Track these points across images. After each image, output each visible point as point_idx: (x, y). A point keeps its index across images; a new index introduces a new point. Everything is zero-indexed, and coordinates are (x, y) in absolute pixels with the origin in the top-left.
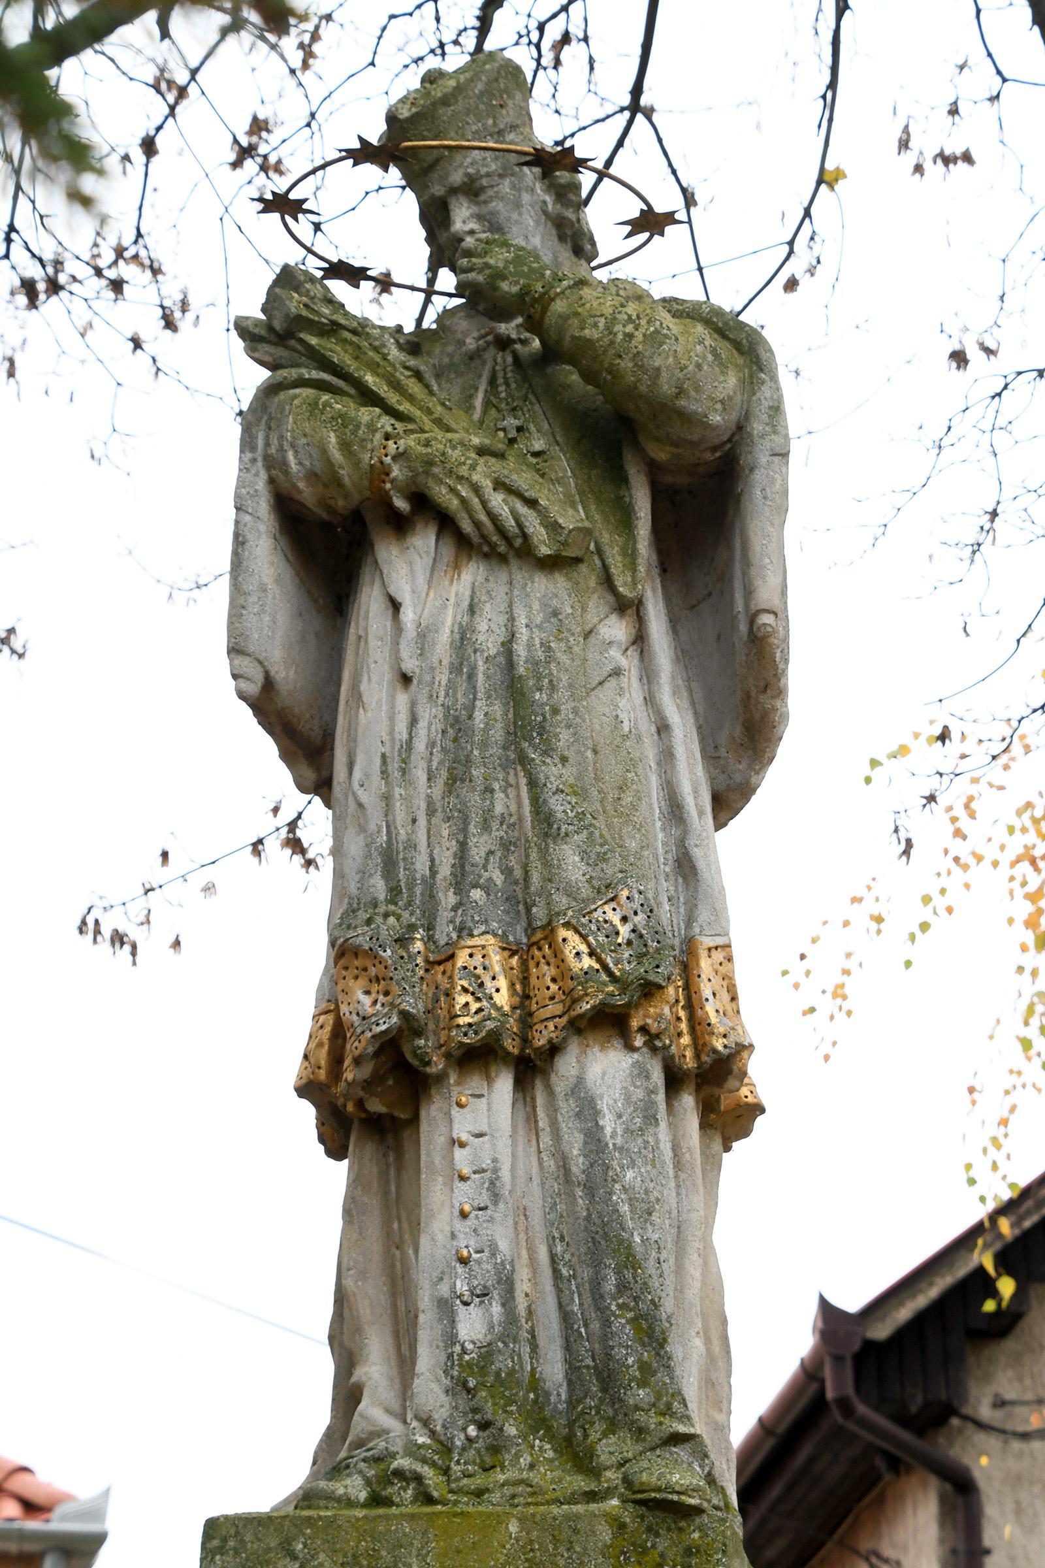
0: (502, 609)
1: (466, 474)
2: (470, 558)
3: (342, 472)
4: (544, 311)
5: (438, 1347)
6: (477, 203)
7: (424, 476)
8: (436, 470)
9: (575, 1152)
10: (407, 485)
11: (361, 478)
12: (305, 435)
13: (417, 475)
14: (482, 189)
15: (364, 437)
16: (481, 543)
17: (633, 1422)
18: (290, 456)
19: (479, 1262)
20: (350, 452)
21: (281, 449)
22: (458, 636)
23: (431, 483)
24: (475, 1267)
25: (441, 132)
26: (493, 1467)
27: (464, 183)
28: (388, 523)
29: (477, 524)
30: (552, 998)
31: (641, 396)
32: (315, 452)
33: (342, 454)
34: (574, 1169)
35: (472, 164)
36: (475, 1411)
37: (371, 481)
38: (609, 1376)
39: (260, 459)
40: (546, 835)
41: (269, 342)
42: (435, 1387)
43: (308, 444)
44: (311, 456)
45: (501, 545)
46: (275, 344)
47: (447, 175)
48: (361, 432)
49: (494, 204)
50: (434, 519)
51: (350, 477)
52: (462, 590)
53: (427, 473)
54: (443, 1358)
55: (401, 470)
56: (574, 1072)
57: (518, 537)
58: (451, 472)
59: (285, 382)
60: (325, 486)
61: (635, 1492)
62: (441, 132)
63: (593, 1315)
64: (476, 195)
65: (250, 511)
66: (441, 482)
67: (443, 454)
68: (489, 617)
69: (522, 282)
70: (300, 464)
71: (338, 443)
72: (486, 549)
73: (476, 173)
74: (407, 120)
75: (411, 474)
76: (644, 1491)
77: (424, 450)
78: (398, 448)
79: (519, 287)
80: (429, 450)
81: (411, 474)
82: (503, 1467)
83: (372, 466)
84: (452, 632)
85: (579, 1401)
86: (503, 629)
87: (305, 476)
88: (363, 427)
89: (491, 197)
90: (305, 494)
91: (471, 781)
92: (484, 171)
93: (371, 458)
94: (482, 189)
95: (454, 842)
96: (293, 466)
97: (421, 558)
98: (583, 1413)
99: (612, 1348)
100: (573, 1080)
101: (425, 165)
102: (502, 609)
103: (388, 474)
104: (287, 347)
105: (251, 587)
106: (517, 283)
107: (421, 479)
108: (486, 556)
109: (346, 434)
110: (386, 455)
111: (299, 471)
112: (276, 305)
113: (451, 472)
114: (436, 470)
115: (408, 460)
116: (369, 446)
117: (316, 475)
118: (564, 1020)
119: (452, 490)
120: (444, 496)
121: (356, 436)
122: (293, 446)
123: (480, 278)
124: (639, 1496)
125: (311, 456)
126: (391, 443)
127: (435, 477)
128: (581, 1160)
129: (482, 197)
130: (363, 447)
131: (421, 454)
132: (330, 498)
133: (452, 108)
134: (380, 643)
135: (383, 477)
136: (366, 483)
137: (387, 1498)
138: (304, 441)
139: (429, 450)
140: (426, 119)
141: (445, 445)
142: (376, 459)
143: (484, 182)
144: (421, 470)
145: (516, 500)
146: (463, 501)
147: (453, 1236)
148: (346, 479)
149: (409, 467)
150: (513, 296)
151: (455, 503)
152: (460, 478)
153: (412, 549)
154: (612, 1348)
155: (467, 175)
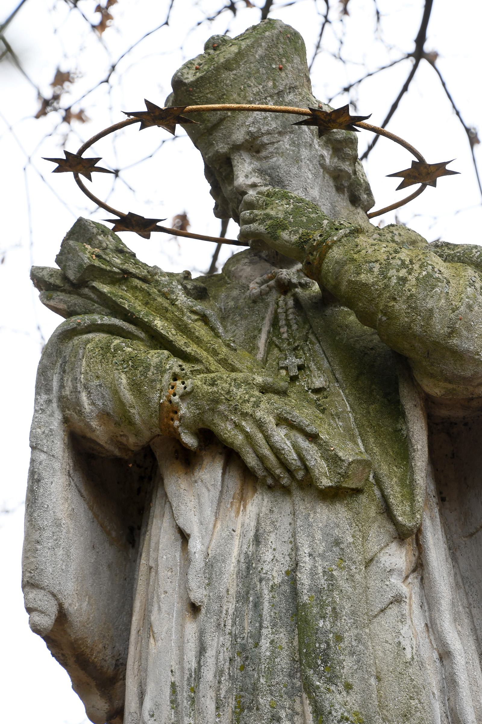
0: (286, 539)
1: (250, 411)
2: (255, 491)
3: (132, 411)
4: (322, 258)
6: (260, 159)
7: (210, 413)
8: (222, 407)
10: (195, 421)
11: (151, 416)
12: (98, 377)
13: (203, 412)
14: (264, 146)
15: (153, 377)
16: (265, 476)
18: (84, 396)
20: (141, 393)
21: (75, 391)
22: (244, 566)
23: (217, 420)
25: (224, 94)
27: (246, 140)
28: (177, 458)
32: (107, 393)
33: (133, 395)
35: (253, 123)
37: (160, 419)
39: (55, 400)
43: (100, 386)
44: (103, 397)
45: (284, 478)
46: (70, 293)
47: (231, 134)
48: (150, 373)
49: (275, 159)
50: (221, 454)
51: (140, 416)
52: (247, 521)
55: (188, 408)
57: (301, 469)
58: (236, 409)
59: (79, 328)
60: (117, 424)
62: (224, 94)
64: (258, 152)
65: (45, 449)
66: (227, 418)
67: (228, 392)
68: (273, 547)
69: (301, 231)
70: (93, 404)
71: (129, 384)
72: (270, 481)
73: (257, 131)
74: (192, 84)
75: (198, 412)
77: (210, 389)
78: (185, 388)
79: (298, 236)
80: (215, 389)
81: (198, 412)
83: (161, 405)
84: (239, 561)
86: (288, 558)
87: (97, 416)
88: (152, 369)
89: (272, 152)
90: (98, 432)
92: (264, 129)
93: (160, 397)
94: (264, 146)
96: (86, 406)
97: (209, 490)
101: (209, 125)
102: (286, 539)
103: (176, 412)
105: (46, 523)
107: (208, 416)
109: (136, 376)
110: (175, 395)
111: (92, 411)
112: (70, 256)
113: (236, 409)
114: (222, 407)
115: (195, 398)
116: (158, 386)
117: (108, 414)
119: (237, 426)
120: (229, 432)
121: (146, 377)
122: (86, 387)
123: (262, 228)
125: (103, 397)
126: (178, 383)
129: (264, 154)
130: (153, 388)
131: (207, 393)
132: (121, 436)
133: (234, 72)
134: (169, 573)
135: (172, 415)
136: (155, 421)
139: (215, 389)
140: (210, 83)
141: (230, 384)
142: (165, 398)
143: (265, 139)
144: (207, 408)
145: (298, 435)
148: (137, 417)
149: (196, 405)
150: (293, 244)
152: (244, 415)
153: (200, 483)
155: (249, 133)
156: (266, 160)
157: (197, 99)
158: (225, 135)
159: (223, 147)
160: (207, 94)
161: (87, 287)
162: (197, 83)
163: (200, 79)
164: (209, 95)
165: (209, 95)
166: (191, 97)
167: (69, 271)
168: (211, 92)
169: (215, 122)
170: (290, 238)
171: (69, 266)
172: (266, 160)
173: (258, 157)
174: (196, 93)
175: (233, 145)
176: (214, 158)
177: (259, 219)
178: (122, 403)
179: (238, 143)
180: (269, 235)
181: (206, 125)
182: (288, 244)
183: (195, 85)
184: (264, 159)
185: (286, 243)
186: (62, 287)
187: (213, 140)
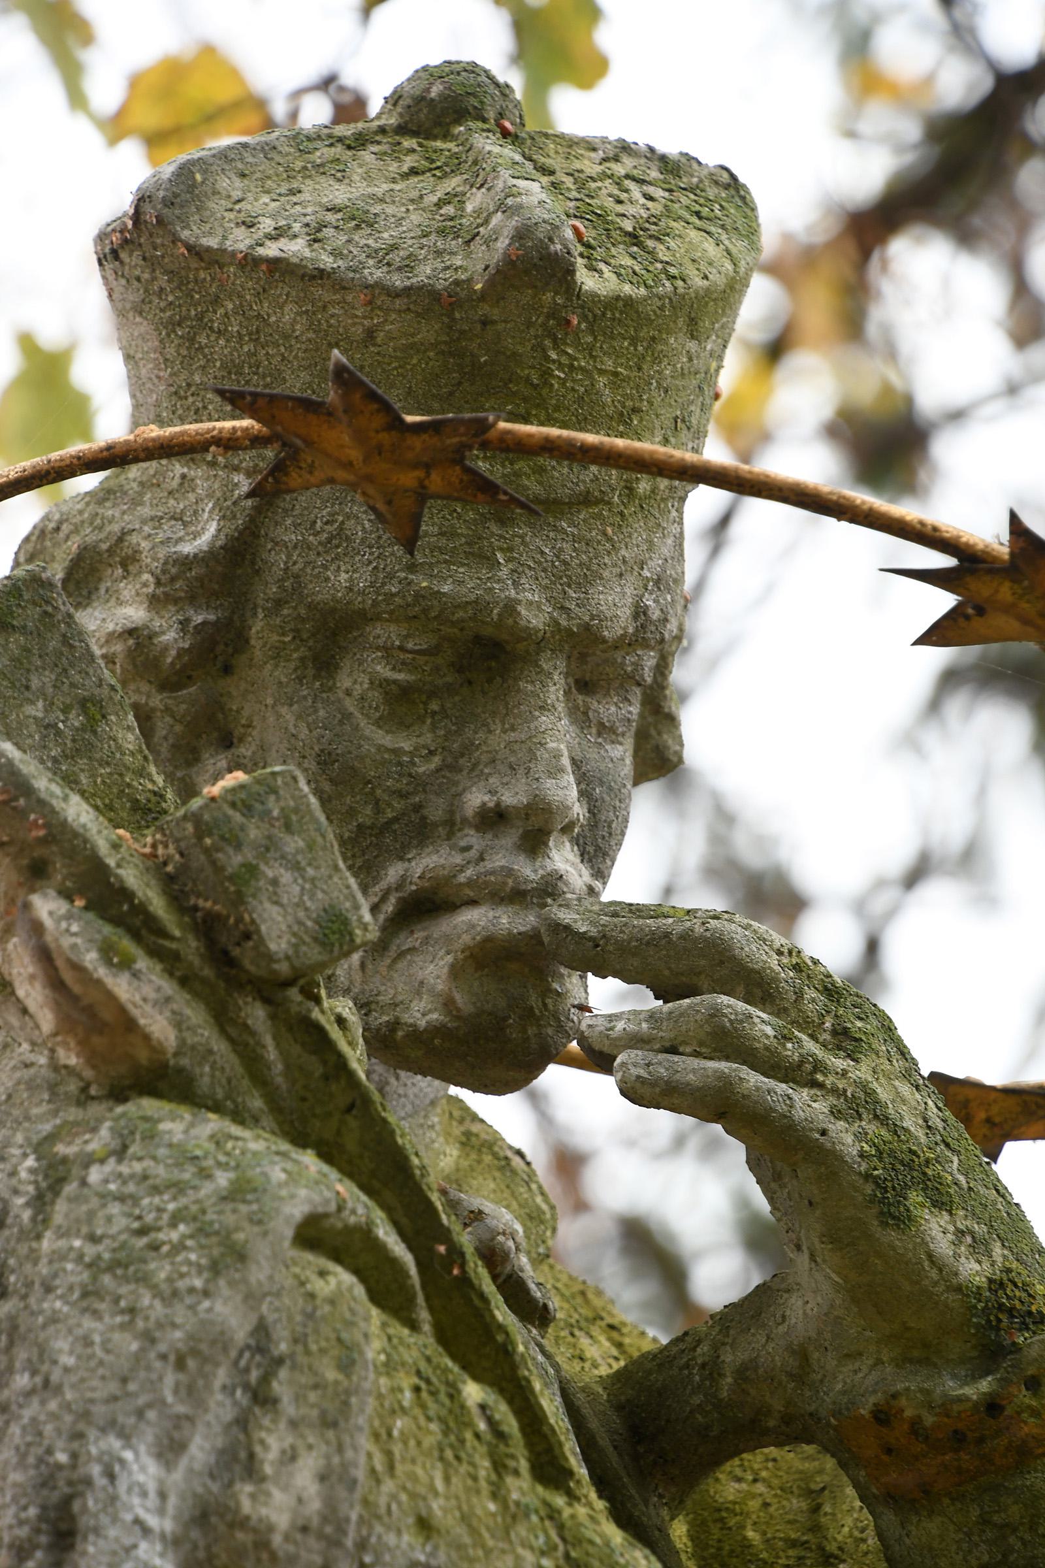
106: (979, 1247)
112: (293, 844)
140: (634, 341)
150: (959, 1289)
156: (599, 734)
157: (561, 367)
158: (565, 563)
159: (539, 606)
160: (602, 372)
161: (267, 1001)
162: (604, 314)
163: (620, 304)
164: (602, 381)
165: (602, 381)
166: (548, 343)
167: (267, 905)
168: (616, 374)
169: (563, 493)
170: (956, 1256)
171: (275, 882)
172: (599, 734)
173: (577, 708)
174: (577, 344)
175: (587, 627)
176: (460, 614)
177: (834, 1091)
179: (606, 633)
180: (869, 1189)
181: (517, 474)
182: (934, 1274)
183: (595, 316)
184: (594, 730)
185: (926, 1264)
186: (172, 938)
187: (501, 549)
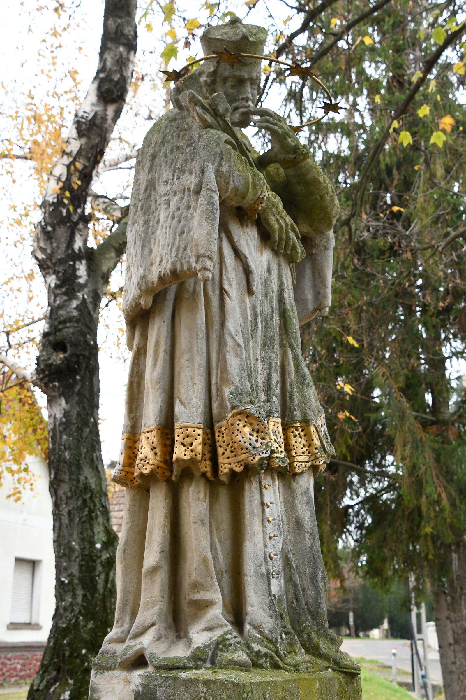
4: (304, 159)
5: (264, 595)
8: (274, 209)
9: (307, 519)
12: (239, 171)
17: (328, 635)
19: (276, 559)
22: (264, 281)
23: (270, 214)
24: (275, 562)
26: (291, 652)
29: (281, 238)
30: (303, 453)
31: (326, 211)
34: (306, 526)
36: (284, 627)
37: (255, 203)
38: (317, 614)
40: (302, 383)
41: (210, 113)
42: (262, 612)
44: (240, 182)
53: (271, 209)
54: (267, 601)
56: (306, 485)
61: (341, 668)
63: (310, 587)
76: (347, 669)
82: (296, 653)
85: (304, 622)
91: (273, 348)
93: (261, 194)
95: (265, 373)
98: (305, 627)
99: (320, 603)
100: (305, 488)
103: (261, 203)
104: (216, 120)
106: (294, 142)
107: (268, 210)
108: (273, 250)
112: (222, 101)
117: (237, 190)
118: (308, 464)
119: (277, 220)
123: (280, 131)
124: (345, 670)
125: (240, 182)
127: (272, 212)
128: (310, 523)
136: (252, 202)
137: (260, 664)
138: (237, 173)
146: (281, 227)
147: (265, 546)
151: (276, 226)
154: (320, 603)
178: (248, 188)
